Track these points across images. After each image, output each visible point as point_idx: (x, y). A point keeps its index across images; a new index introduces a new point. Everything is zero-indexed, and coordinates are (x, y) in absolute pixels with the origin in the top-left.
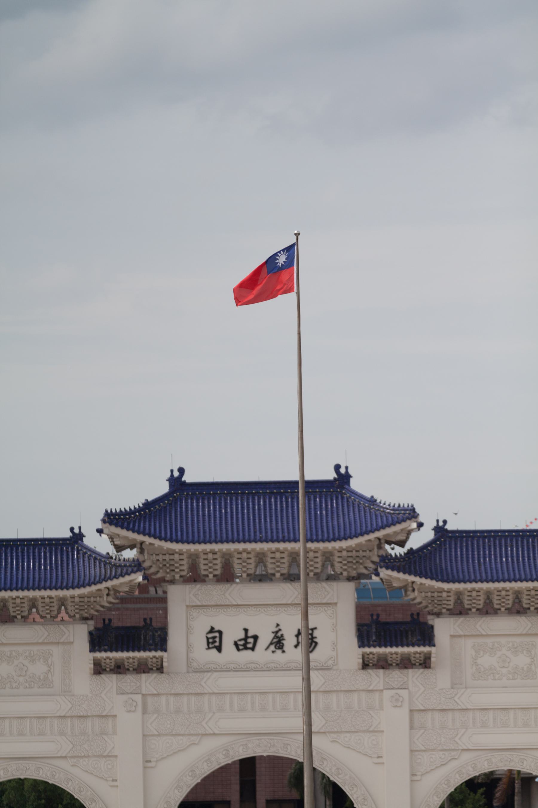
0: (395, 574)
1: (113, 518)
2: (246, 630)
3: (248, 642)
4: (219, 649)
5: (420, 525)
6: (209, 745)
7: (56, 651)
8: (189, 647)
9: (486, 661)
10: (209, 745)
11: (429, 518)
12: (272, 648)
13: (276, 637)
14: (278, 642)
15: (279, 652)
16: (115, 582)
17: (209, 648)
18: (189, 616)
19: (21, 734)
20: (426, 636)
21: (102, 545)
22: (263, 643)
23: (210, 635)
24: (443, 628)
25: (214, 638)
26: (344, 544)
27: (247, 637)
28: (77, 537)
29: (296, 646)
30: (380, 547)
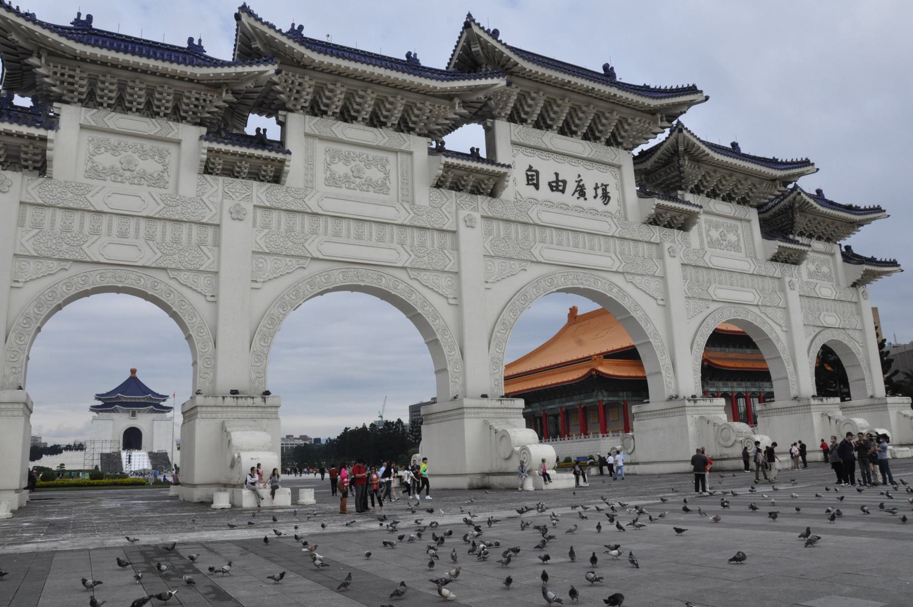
2: (557, 174)
3: (557, 185)
4: (537, 186)
5: (707, 98)
12: (577, 194)
13: (579, 186)
14: (581, 191)
15: (582, 198)
17: (528, 184)
23: (529, 173)
25: (532, 176)
27: (557, 181)
29: (595, 197)
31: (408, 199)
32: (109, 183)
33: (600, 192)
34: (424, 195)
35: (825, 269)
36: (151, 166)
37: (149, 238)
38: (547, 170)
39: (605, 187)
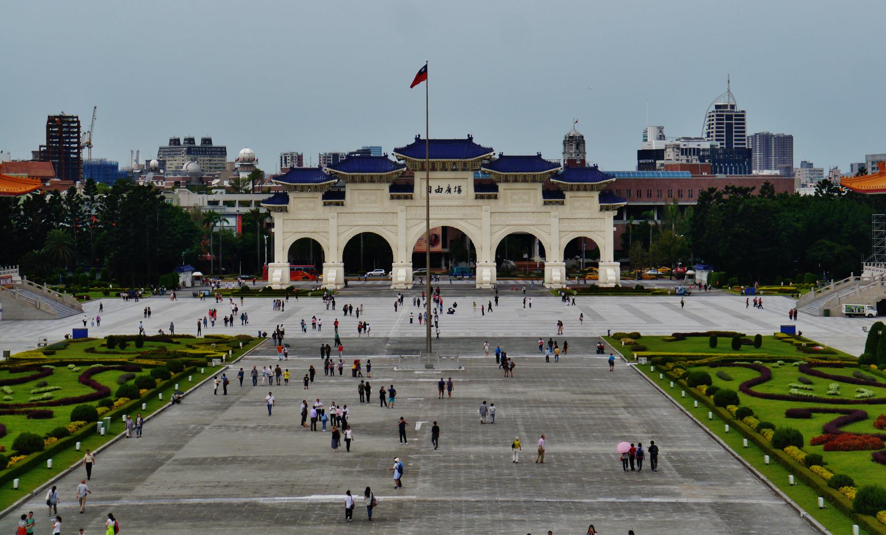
1: (396, 150)
3: (439, 190)
14: (449, 190)
20: (496, 189)
21: (393, 159)
22: (444, 191)
24: (502, 186)
35: (588, 204)
36: (311, 205)
39: (459, 187)
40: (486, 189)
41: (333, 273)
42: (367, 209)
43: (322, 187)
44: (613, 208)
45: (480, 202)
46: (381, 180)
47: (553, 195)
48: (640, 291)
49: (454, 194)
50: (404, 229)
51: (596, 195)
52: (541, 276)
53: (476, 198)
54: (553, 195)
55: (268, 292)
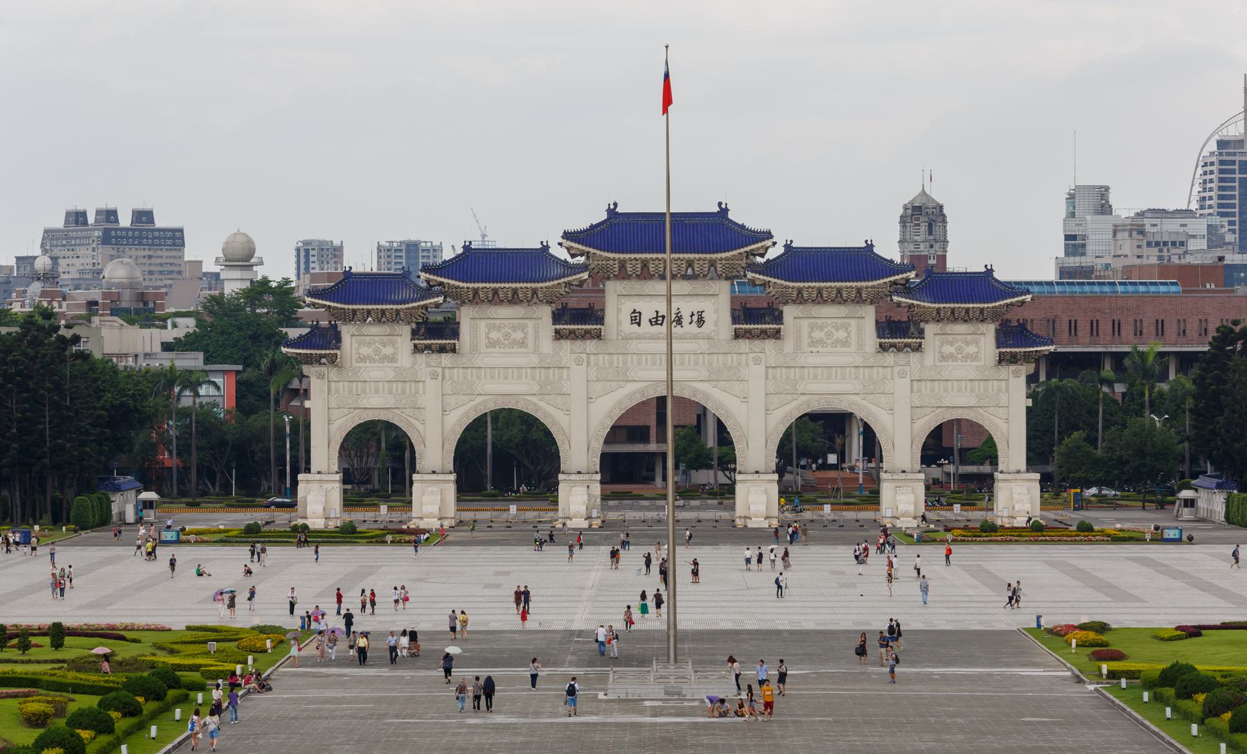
0: (757, 276)
1: (568, 235)
4: (639, 324)
6: (631, 387)
7: (530, 323)
8: (619, 323)
9: (817, 334)
10: (631, 387)
11: (780, 239)
16: (570, 278)
18: (619, 302)
19: (506, 378)
20: (779, 319)
21: (562, 254)
24: (789, 312)
26: (724, 255)
28: (545, 248)
30: (747, 257)
31: (536, 350)
32: (368, 364)
33: (695, 318)
34: (547, 344)
35: (972, 349)
36: (388, 351)
37: (390, 392)
38: (648, 309)
40: (756, 318)
41: (433, 498)
42: (506, 361)
43: (410, 313)
44: (1027, 358)
45: (744, 345)
46: (533, 298)
47: (898, 331)
48: (1086, 533)
49: (689, 328)
50: (581, 402)
51: (990, 329)
52: (873, 499)
53: (737, 335)
54: (898, 331)
55: (303, 536)
